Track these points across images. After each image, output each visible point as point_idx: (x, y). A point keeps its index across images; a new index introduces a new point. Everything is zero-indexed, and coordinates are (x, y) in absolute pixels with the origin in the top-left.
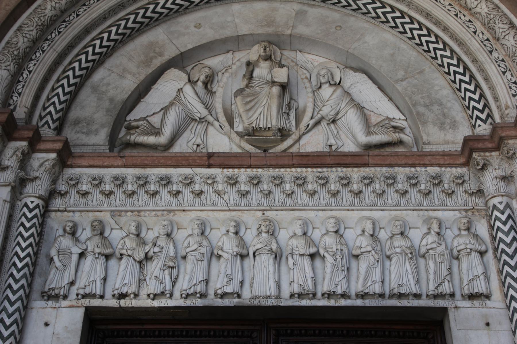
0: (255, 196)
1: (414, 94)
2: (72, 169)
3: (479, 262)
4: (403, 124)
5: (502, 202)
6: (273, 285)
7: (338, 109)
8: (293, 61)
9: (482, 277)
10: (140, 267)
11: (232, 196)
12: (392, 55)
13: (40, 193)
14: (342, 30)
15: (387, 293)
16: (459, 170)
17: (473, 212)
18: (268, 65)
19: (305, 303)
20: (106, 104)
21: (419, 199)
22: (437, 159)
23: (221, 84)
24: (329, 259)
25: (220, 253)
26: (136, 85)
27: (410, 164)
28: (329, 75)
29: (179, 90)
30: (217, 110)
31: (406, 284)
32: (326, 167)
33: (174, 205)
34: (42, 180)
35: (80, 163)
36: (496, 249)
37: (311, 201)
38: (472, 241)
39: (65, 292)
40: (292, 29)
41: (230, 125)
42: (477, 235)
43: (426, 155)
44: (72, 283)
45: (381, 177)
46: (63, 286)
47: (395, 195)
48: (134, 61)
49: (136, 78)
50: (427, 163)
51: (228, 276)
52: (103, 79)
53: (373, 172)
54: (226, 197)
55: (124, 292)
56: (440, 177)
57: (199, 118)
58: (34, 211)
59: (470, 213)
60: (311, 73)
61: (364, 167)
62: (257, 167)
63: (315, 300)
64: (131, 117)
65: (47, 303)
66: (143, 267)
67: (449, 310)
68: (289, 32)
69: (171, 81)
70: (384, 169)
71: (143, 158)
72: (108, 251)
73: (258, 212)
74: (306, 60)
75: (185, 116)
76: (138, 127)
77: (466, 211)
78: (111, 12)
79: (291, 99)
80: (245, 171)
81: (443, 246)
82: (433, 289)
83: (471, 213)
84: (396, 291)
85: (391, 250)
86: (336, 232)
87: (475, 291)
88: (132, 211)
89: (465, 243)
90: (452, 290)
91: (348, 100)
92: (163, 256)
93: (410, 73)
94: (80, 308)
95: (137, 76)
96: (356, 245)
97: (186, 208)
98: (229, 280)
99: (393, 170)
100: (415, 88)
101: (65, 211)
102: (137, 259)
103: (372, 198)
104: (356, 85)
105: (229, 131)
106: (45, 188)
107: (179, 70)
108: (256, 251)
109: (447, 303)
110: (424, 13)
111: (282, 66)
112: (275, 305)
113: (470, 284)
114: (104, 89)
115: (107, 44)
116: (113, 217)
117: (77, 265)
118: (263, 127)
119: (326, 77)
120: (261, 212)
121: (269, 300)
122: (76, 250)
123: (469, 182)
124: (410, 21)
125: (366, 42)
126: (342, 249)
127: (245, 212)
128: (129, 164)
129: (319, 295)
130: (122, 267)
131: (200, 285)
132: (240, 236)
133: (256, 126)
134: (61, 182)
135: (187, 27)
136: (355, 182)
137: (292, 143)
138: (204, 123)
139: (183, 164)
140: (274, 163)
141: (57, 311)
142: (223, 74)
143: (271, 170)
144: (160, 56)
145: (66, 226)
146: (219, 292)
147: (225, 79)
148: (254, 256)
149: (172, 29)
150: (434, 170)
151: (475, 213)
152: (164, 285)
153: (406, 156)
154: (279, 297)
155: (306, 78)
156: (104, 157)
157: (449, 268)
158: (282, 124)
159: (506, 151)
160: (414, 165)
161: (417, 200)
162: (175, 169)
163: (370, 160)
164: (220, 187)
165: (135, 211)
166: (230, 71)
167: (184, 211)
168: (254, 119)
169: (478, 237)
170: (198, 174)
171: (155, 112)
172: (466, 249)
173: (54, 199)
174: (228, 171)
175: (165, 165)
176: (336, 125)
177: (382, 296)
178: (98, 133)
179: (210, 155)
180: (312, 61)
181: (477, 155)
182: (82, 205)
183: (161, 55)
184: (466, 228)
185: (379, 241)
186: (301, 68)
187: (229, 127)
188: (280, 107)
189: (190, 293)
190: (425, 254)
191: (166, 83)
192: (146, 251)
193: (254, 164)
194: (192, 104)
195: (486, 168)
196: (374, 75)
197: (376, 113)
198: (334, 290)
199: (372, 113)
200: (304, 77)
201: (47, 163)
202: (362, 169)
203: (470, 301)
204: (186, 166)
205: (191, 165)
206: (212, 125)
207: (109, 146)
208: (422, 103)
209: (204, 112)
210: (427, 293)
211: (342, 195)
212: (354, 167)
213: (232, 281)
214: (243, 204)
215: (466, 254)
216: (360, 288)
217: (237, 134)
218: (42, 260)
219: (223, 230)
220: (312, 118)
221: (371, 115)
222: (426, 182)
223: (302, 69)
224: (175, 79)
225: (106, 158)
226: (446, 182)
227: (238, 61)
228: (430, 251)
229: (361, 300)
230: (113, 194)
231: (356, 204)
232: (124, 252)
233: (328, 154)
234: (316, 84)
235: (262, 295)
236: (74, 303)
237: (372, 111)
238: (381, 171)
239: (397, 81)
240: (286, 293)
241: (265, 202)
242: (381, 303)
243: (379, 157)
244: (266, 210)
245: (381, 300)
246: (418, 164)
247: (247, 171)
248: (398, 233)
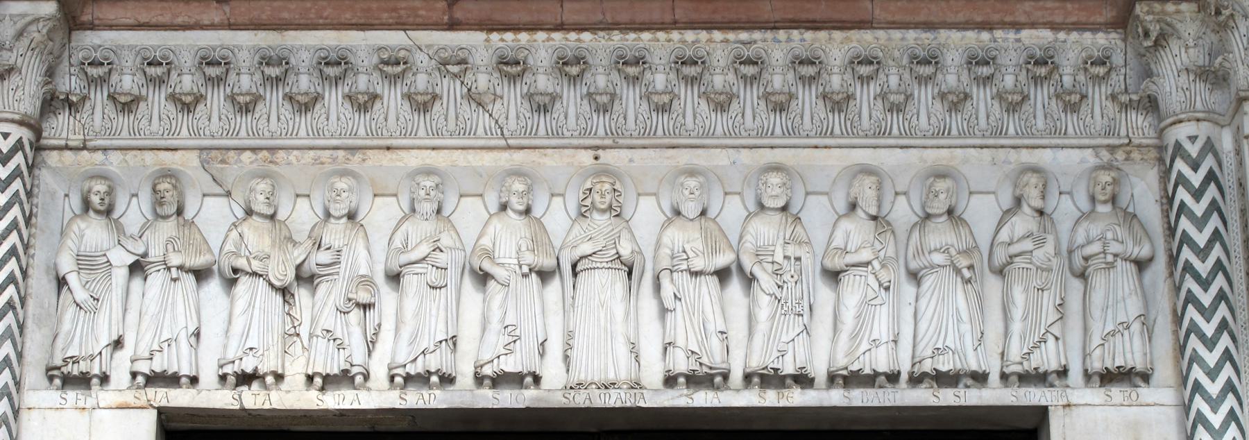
0: (572, 102)
2: (94, 32)
3: (1132, 287)
5: (1196, 137)
6: (622, 350)
9: (1136, 327)
10: (285, 301)
11: (511, 103)
13: (22, 110)
15: (905, 368)
16: (1101, 39)
17: (1129, 153)
19: (703, 399)
21: (998, 116)
22: (1047, 9)
24: (766, 280)
25: (487, 266)
27: (978, 23)
31: (953, 348)
32: (760, 28)
33: (362, 132)
34: (24, 71)
35: (112, 17)
36: (1173, 259)
37: (720, 123)
38: (1121, 232)
39: (104, 370)
42: (1135, 216)
44: (118, 344)
45: (902, 56)
46: (97, 352)
47: (938, 105)
50: (1023, 19)
51: (510, 329)
53: (882, 42)
54: (497, 109)
55: (249, 370)
56: (1052, 57)
58: (12, 161)
59: (1120, 155)
61: (860, 28)
62: (580, 28)
63: (729, 392)
65: (64, 396)
66: (291, 301)
67: (1050, 414)
70: (911, 34)
72: (199, 261)
73: (583, 150)
77: (1112, 149)
80: (549, 39)
81: (1049, 248)
82: (1018, 359)
83: (1124, 157)
84: (927, 366)
85: (922, 258)
86: (784, 209)
87: (1117, 364)
88: (254, 150)
89: (1103, 239)
90: (1063, 362)
92: (341, 274)
94: (144, 410)
96: (834, 245)
97: (394, 142)
98: (511, 339)
99: (936, 38)
101: (84, 148)
102: (277, 284)
103: (878, 113)
106: (32, 92)
108: (579, 261)
109: (1048, 395)
112: (628, 405)
113: (1106, 345)
116: (206, 166)
117: (124, 295)
120: (591, 153)
121: (612, 391)
122: (120, 259)
123: (1123, 71)
126: (797, 255)
127: (549, 151)
128: (240, 20)
129: (737, 376)
130: (240, 304)
131: (438, 351)
132: (535, 218)
134: (67, 69)
136: (836, 70)
139: (384, 21)
140: (624, 17)
141: (90, 416)
143: (617, 36)
145: (89, 191)
146: (487, 370)
148: (575, 274)
150: (1038, 37)
151: (1132, 155)
152: (347, 353)
154: (636, 385)
157: (1059, 305)
159: (1213, 9)
160: (989, 24)
161: (992, 118)
162: (361, 33)
163: (877, 12)
164: (482, 82)
165: (261, 149)
167: (388, 148)
169: (1135, 221)
170: (423, 48)
172: (1104, 252)
173: (52, 115)
174: (502, 40)
175: (335, 22)
177: (893, 378)
181: (1146, 9)
182: (125, 133)
184: (1106, 197)
185: (893, 232)
189: (413, 373)
190: (1005, 266)
192: (299, 261)
193: (571, 21)
195: (1165, 44)
198: (775, 366)
201: (33, 28)
202: (855, 34)
203: (1103, 390)
204: (390, 25)
205: (404, 24)
210: (1002, 367)
211: (800, 104)
213: (518, 342)
214: (542, 131)
215: (1104, 266)
216: (841, 361)
218: (40, 284)
219: (493, 202)
222: (1018, 69)
226: (1065, 72)
228: (1017, 259)
229: (841, 391)
230: (203, 100)
231: (837, 131)
232: (241, 263)
235: (596, 380)
236: (129, 397)
238: (903, 39)
240: (653, 374)
241: (600, 123)
242: (891, 397)
244: (604, 148)
245: (890, 390)
246: (998, 24)
247: (553, 39)
248: (941, 211)
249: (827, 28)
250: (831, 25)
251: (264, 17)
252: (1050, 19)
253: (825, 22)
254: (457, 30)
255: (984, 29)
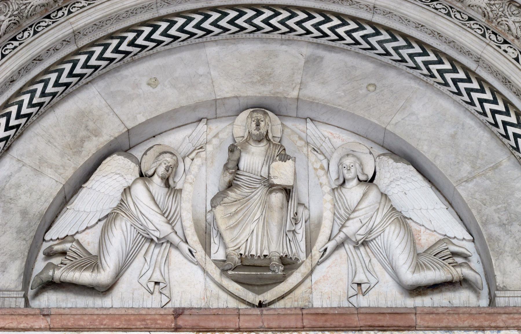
1: (485, 205)
4: (469, 248)
7: (370, 226)
8: (300, 138)
12: (453, 137)
14: (378, 91)
18: (263, 149)
20: (16, 220)
22: (515, 319)
23: (190, 177)
26: (61, 186)
27: (476, 327)
28: (357, 165)
29: (125, 189)
30: (183, 224)
32: (352, 330)
40: (300, 89)
41: (205, 250)
43: (500, 313)
48: (56, 144)
49: (60, 174)
50: (501, 324)
52: (10, 176)
57: (157, 238)
60: (329, 158)
61: (409, 330)
64: (53, 234)
68: (294, 94)
69: (112, 175)
71: (76, 317)
74: (321, 135)
75: (135, 235)
76: (64, 253)
78: (22, 72)
79: (300, 204)
91: (385, 211)
93: (479, 168)
95: (61, 171)
100: (487, 195)
104: (399, 183)
105: (204, 260)
107: (125, 157)
110: (500, 77)
111: (284, 157)
114: (11, 194)
115: (17, 122)
118: (257, 254)
119: (353, 170)
124: (479, 88)
125: (413, 114)
128: (56, 326)
133: (245, 253)
135: (136, 85)
137: (300, 280)
138: (165, 245)
139: (138, 326)
140: (274, 324)
142: (193, 160)
144: (96, 136)
147: (194, 169)
149: (112, 89)
153: (470, 314)
155: (322, 168)
156: (19, 315)
158: (285, 250)
160: (483, 327)
163: (418, 321)
166: (203, 154)
168: (243, 242)
171: (89, 226)
175: (110, 327)
176: (367, 248)
178: (6, 268)
179: (178, 313)
180: (330, 137)
183: (96, 133)
186: (314, 150)
187: (204, 252)
188: (282, 224)
191: (105, 178)
194: (147, 215)
196: (426, 167)
197: (428, 229)
199: (423, 228)
200: (318, 166)
205: (149, 328)
206: (177, 248)
207: (24, 292)
208: (497, 220)
209: (166, 229)
212: (394, 330)
217: (215, 264)
220: (329, 240)
221: (420, 231)
223: (315, 153)
224: (118, 172)
225: (23, 317)
227: (215, 137)
233: (356, 312)
234: (336, 177)
237: (423, 226)
239: (460, 182)
243: (431, 316)
246: (487, 327)
249: (390, 330)
250: (392, 328)
251: (70, 324)
252: (517, 325)
253: (388, 327)
254: (179, 331)
255: (479, 330)
